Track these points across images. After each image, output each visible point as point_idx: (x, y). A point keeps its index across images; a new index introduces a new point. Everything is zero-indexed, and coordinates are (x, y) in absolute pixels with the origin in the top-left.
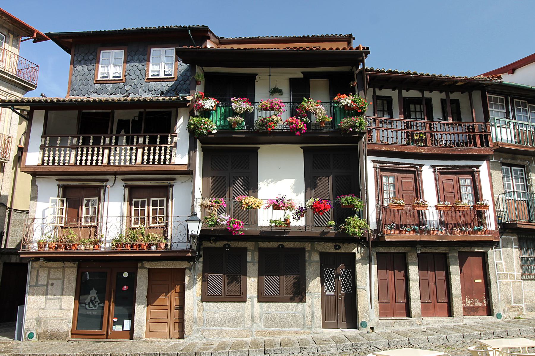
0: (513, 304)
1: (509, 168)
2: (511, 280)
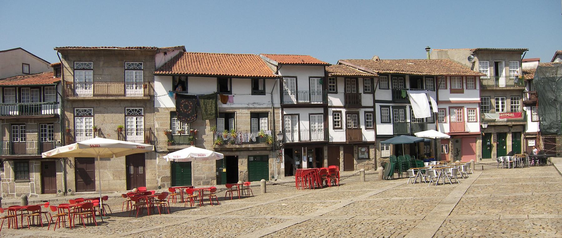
0: (10, 193)
1: (18, 126)
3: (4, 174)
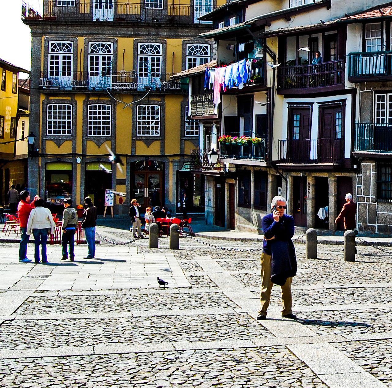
0: (368, 224)
1: (385, 95)
2: (367, 203)
3: (362, 186)
